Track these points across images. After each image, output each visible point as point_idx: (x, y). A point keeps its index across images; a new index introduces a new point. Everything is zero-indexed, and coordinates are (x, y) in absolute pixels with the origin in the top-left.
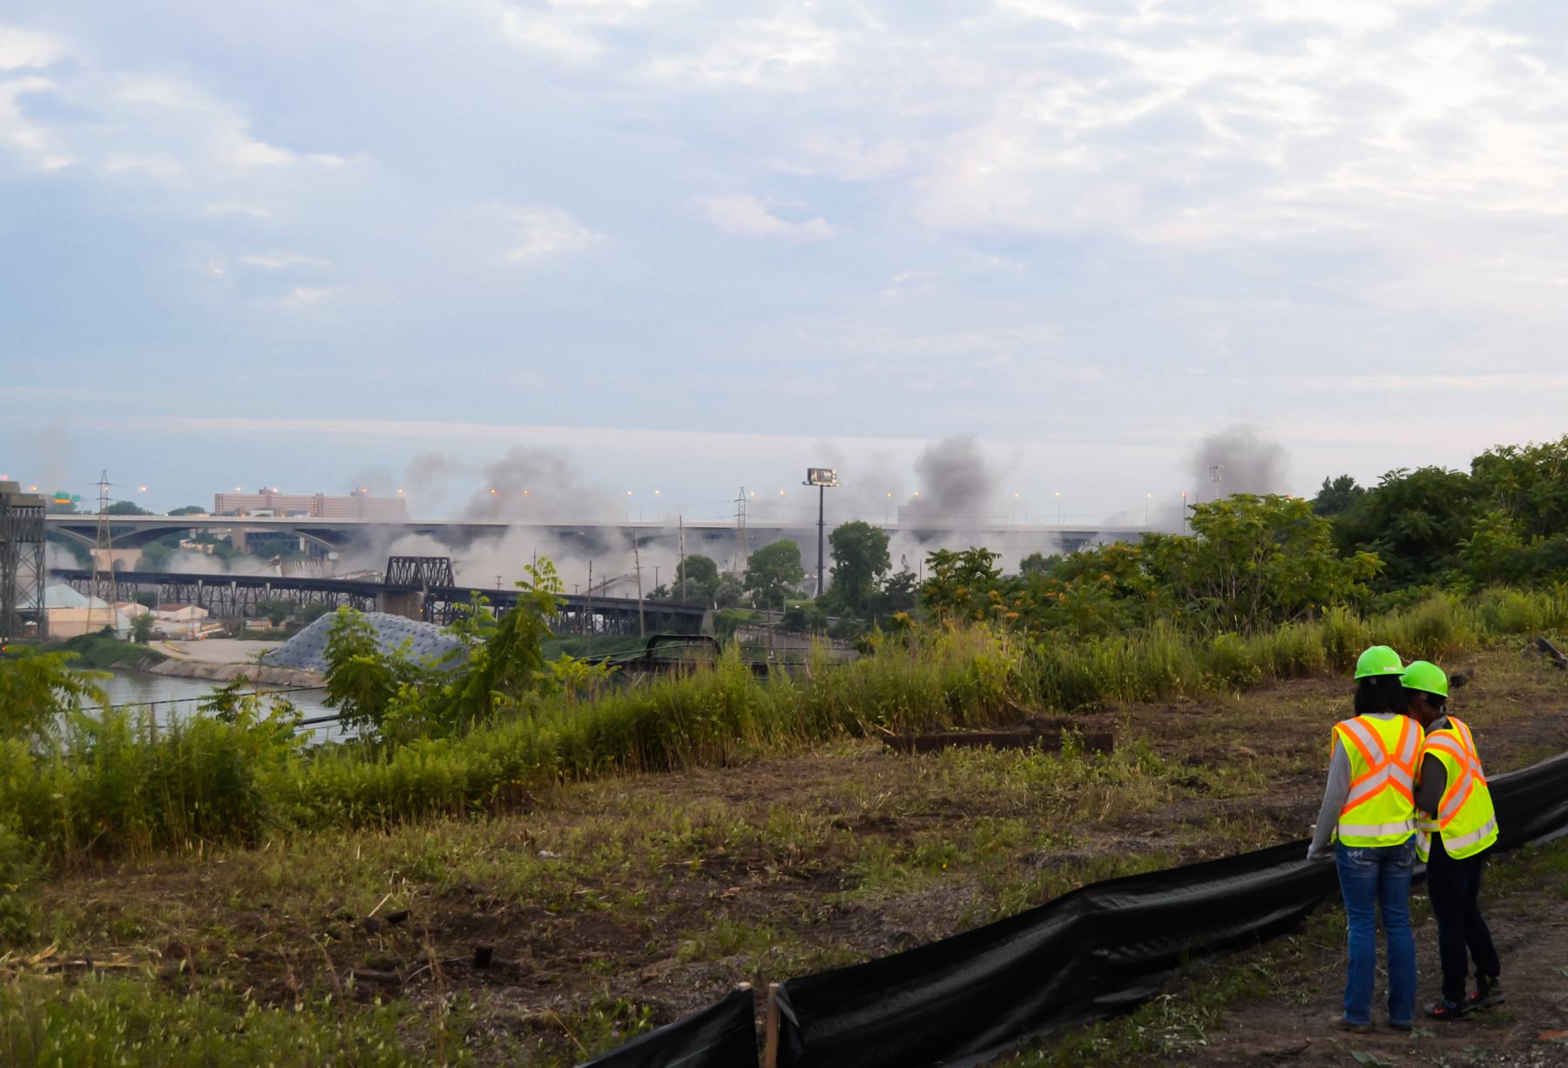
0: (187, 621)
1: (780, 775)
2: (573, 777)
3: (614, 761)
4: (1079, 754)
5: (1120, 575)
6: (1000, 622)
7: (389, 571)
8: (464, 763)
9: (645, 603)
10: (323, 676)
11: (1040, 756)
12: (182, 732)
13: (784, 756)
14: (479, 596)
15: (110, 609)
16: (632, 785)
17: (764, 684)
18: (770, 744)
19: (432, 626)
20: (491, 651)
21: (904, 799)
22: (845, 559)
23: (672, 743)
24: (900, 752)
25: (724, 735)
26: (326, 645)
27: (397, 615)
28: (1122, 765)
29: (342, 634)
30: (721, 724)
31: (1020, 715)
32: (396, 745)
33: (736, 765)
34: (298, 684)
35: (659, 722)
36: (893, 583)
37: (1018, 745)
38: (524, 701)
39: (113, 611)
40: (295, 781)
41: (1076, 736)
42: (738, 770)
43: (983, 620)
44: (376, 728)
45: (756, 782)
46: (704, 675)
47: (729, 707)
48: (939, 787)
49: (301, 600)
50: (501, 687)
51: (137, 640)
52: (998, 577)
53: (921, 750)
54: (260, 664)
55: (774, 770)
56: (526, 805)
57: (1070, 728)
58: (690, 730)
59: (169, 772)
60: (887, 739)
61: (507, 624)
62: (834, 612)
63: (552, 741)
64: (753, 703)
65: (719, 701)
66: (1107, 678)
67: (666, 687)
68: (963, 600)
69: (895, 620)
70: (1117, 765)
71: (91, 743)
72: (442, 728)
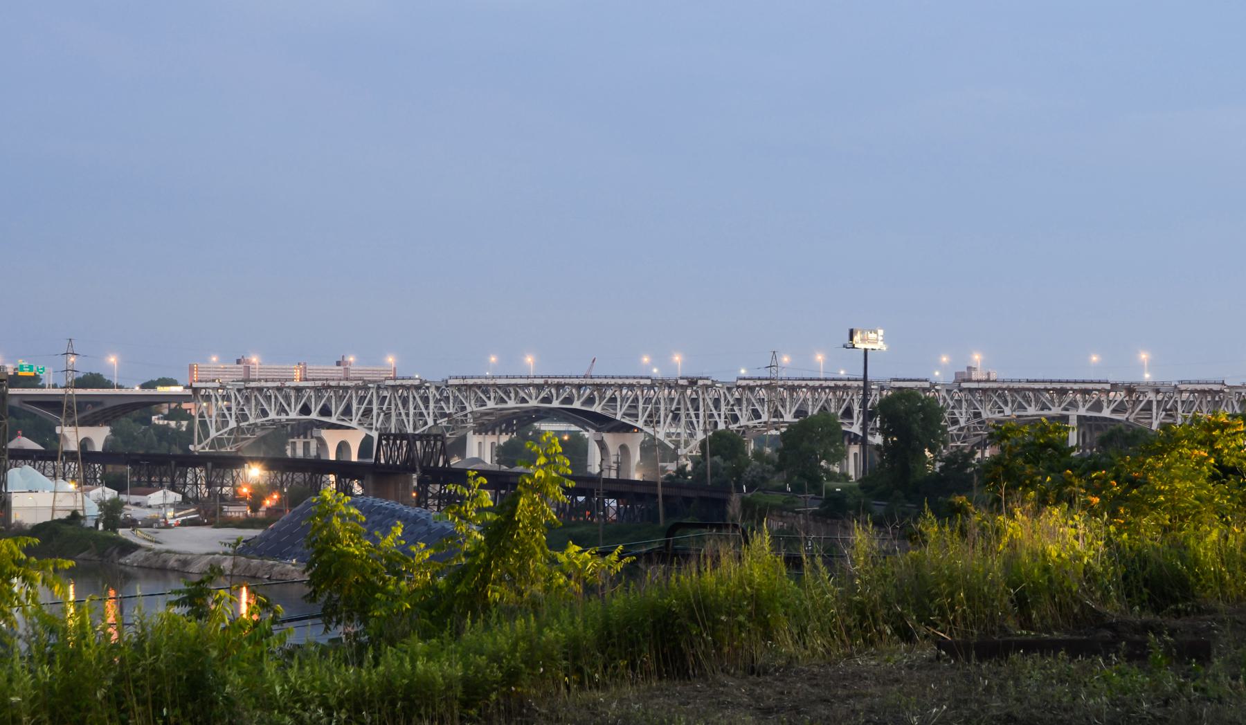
0: (159, 507)
1: (817, 685)
2: (581, 684)
3: (627, 667)
4: (1170, 665)
6: (1076, 506)
10: (303, 567)
11: (1124, 665)
12: (149, 629)
13: (822, 662)
14: (475, 477)
16: (649, 695)
18: (806, 648)
21: (962, 715)
22: (893, 434)
23: (693, 647)
24: (957, 660)
25: (753, 636)
30: (751, 625)
31: (1098, 616)
32: (383, 646)
33: (766, 673)
34: (279, 577)
36: (949, 461)
37: (1097, 652)
38: (526, 595)
39: (79, 495)
40: (272, 687)
41: (1166, 642)
42: (769, 679)
43: (1057, 503)
44: (361, 627)
45: (789, 693)
47: (758, 605)
48: (1002, 701)
49: (282, 483)
51: (106, 527)
52: (1074, 454)
53: (981, 658)
54: (237, 553)
55: (809, 679)
56: (528, 716)
57: (1158, 634)
59: (135, 675)
60: (941, 644)
62: (881, 496)
63: (557, 642)
64: (786, 601)
65: (746, 598)
66: (1203, 574)
67: (686, 579)
68: (1031, 481)
69: (952, 504)
70: (1215, 677)
71: (51, 642)
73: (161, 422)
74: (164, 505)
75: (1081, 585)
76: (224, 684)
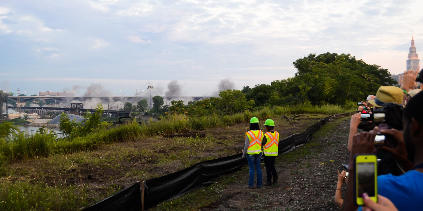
0: (34, 116)
1: (144, 143)
4: (199, 138)
5: (206, 105)
6: (184, 114)
7: (71, 106)
8: (86, 141)
9: (119, 111)
11: (192, 138)
12: (33, 136)
13: (145, 139)
14: (88, 111)
15: (20, 114)
16: (117, 145)
17: (141, 126)
18: (142, 137)
19: (79, 116)
20: (90, 120)
24: (166, 138)
26: (60, 120)
27: (73, 114)
28: (207, 140)
29: (63, 118)
31: (188, 131)
33: (136, 141)
35: (122, 133)
36: (164, 107)
37: (188, 136)
40: (55, 145)
42: (136, 142)
43: (181, 113)
45: (140, 144)
46: (130, 124)
50: (92, 127)
51: (25, 119)
53: (170, 137)
54: (48, 123)
57: (197, 133)
58: (127, 134)
60: (164, 136)
61: (93, 115)
62: (153, 112)
69: (165, 114)
70: (206, 140)
72: (81, 135)
73: (34, 102)
74: (35, 115)
75: (185, 126)
76: (46, 145)
